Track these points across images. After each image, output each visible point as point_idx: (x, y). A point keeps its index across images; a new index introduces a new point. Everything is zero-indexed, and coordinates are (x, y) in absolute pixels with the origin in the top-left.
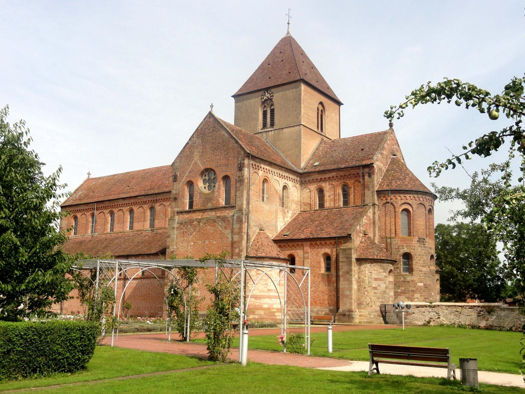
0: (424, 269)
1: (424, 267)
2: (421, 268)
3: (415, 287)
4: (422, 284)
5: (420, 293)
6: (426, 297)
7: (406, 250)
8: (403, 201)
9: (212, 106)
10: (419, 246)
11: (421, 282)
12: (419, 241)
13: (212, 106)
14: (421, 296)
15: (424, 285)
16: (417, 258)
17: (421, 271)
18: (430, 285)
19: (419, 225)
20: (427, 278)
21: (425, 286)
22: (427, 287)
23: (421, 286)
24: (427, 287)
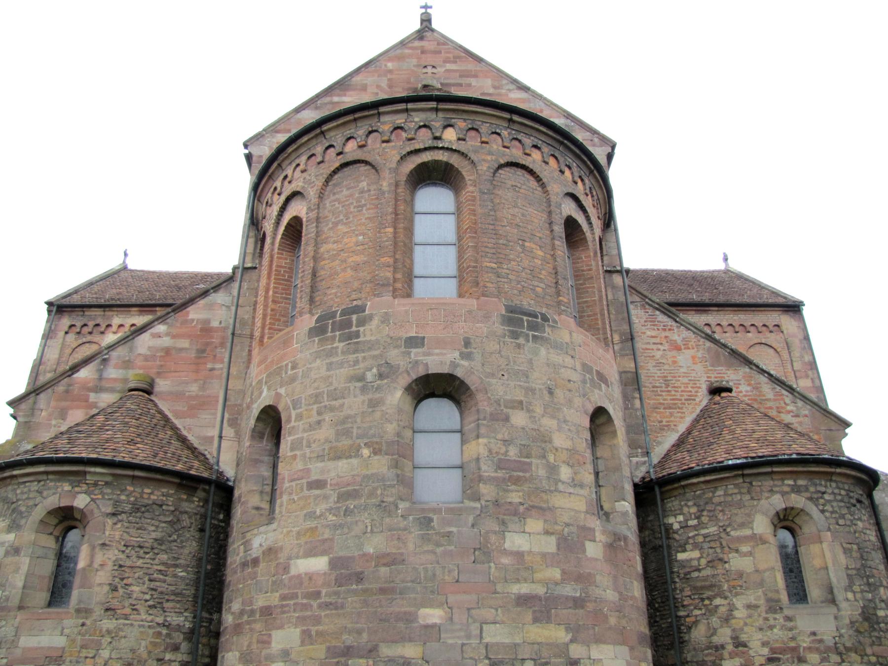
0: (343, 468)
1: (337, 456)
2: (317, 470)
3: (277, 585)
4: (319, 564)
5: (302, 620)
6: (348, 639)
7: (265, 399)
8: (283, 198)
9: (126, 255)
10: (317, 355)
11: (311, 553)
12: (319, 330)
13: (126, 255)
14: (307, 637)
15: (334, 564)
16: (300, 417)
17: (319, 484)
18: (392, 560)
19: (333, 258)
20: (365, 518)
21: (346, 573)
22: (359, 578)
23: (310, 577)
24: (359, 578)
